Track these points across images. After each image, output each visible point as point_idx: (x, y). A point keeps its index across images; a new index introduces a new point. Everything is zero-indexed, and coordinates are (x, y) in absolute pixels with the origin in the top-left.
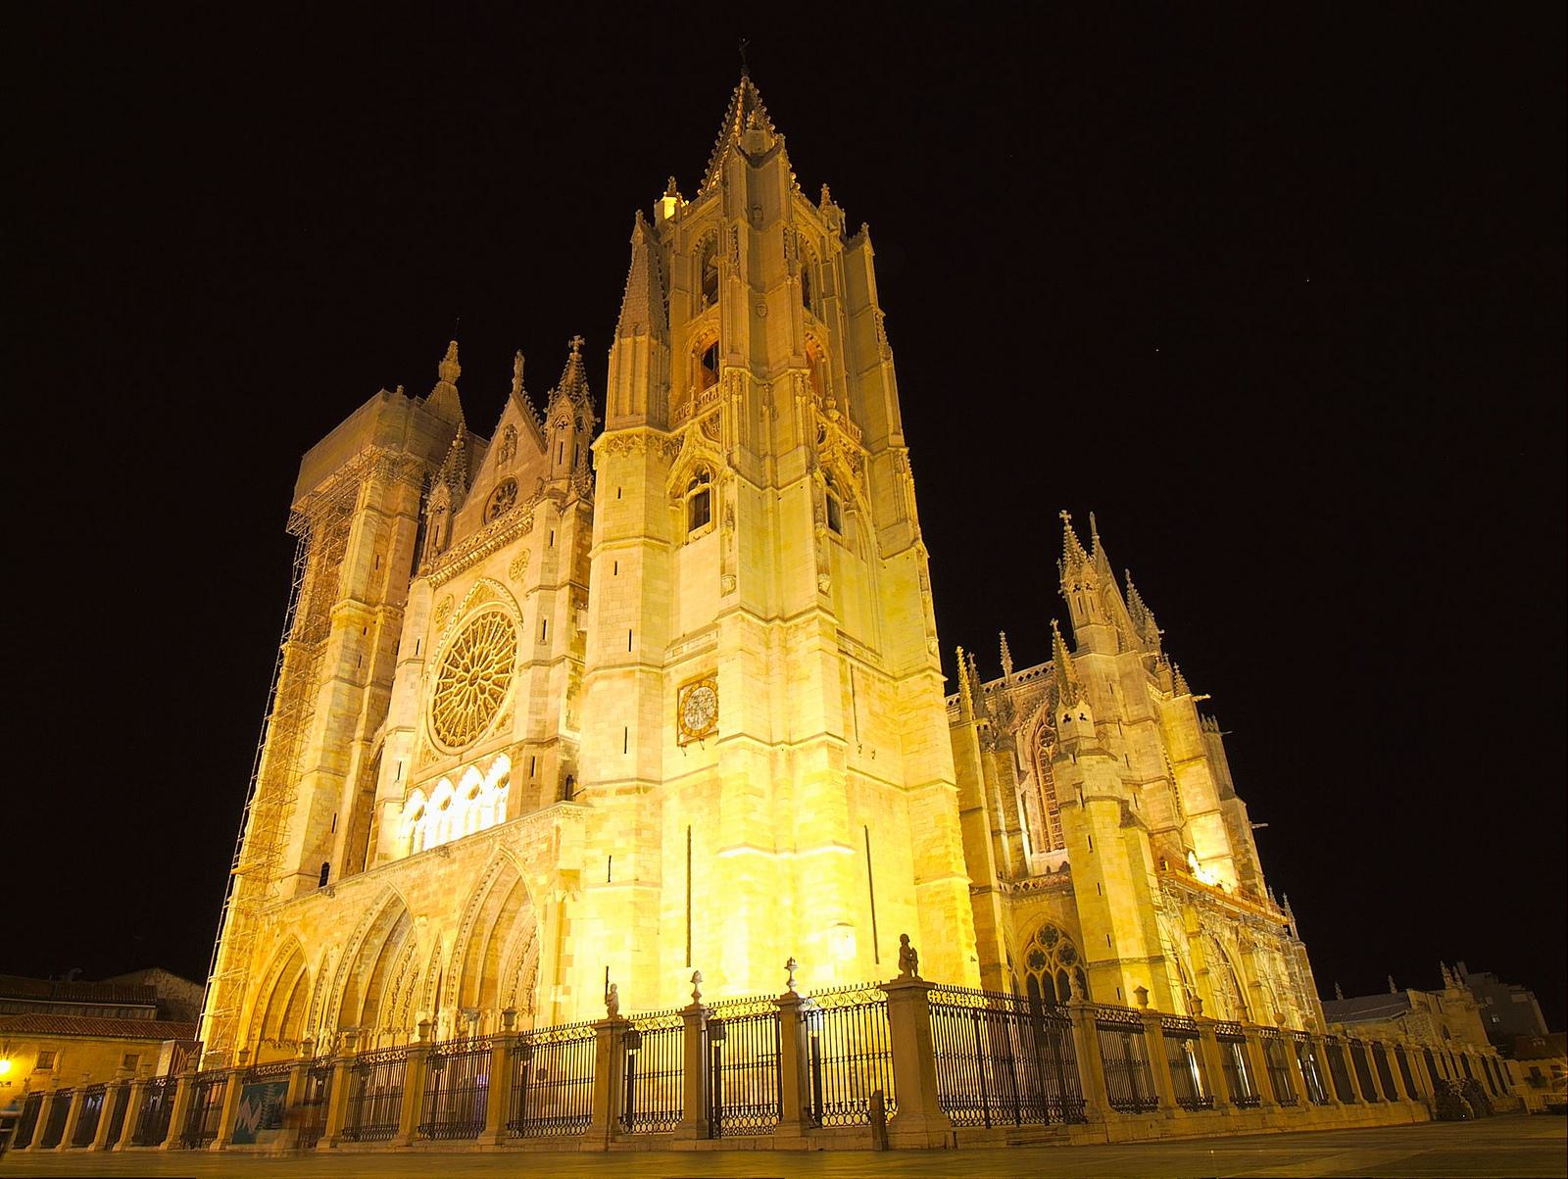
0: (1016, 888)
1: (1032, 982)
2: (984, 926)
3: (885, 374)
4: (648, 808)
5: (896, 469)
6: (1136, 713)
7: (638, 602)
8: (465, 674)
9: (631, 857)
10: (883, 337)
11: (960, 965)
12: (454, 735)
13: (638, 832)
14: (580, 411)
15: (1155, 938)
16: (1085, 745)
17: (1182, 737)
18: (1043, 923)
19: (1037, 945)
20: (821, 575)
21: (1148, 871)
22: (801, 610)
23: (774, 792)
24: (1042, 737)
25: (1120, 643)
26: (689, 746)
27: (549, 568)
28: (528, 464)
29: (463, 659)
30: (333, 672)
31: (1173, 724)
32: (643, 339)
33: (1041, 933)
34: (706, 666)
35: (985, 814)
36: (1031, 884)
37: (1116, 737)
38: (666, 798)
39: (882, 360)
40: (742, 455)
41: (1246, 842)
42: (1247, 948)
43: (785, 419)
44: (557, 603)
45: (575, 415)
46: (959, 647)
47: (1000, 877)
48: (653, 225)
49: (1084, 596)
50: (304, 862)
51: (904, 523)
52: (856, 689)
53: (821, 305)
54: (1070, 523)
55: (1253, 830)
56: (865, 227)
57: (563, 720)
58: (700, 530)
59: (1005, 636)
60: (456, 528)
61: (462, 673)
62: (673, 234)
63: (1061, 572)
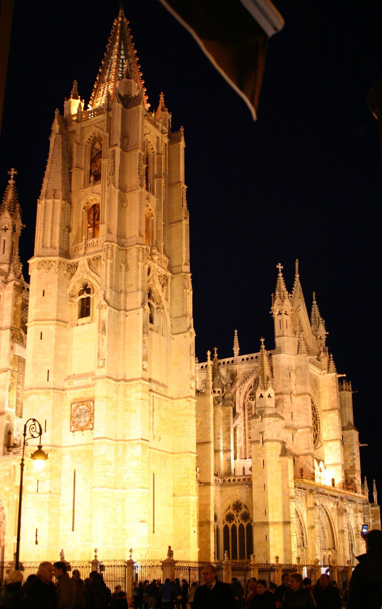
0: (224, 481)
1: (226, 528)
2: (204, 502)
3: (184, 228)
5: (184, 285)
6: (300, 389)
7: (52, 356)
10: (185, 204)
11: (189, 534)
13: (51, 470)
14: (15, 221)
15: (288, 513)
16: (268, 411)
17: (328, 397)
18: (235, 500)
19: (231, 511)
20: (144, 362)
21: (289, 480)
22: (134, 377)
24: (250, 395)
25: (298, 348)
26: (76, 432)
31: (324, 389)
32: (59, 202)
33: (234, 505)
34: (86, 394)
35: (212, 446)
36: (232, 480)
37: (288, 403)
39: (183, 219)
40: (111, 295)
41: (354, 454)
42: (341, 512)
43: (133, 272)
44: (3, 338)
46: (209, 351)
48: (63, 116)
49: (283, 319)
51: (185, 318)
52: (155, 407)
53: (153, 183)
54: (282, 272)
55: (360, 447)
56: (182, 129)
57: (7, 403)
58: (85, 320)
59: (238, 333)
62: (75, 127)
63: (273, 302)
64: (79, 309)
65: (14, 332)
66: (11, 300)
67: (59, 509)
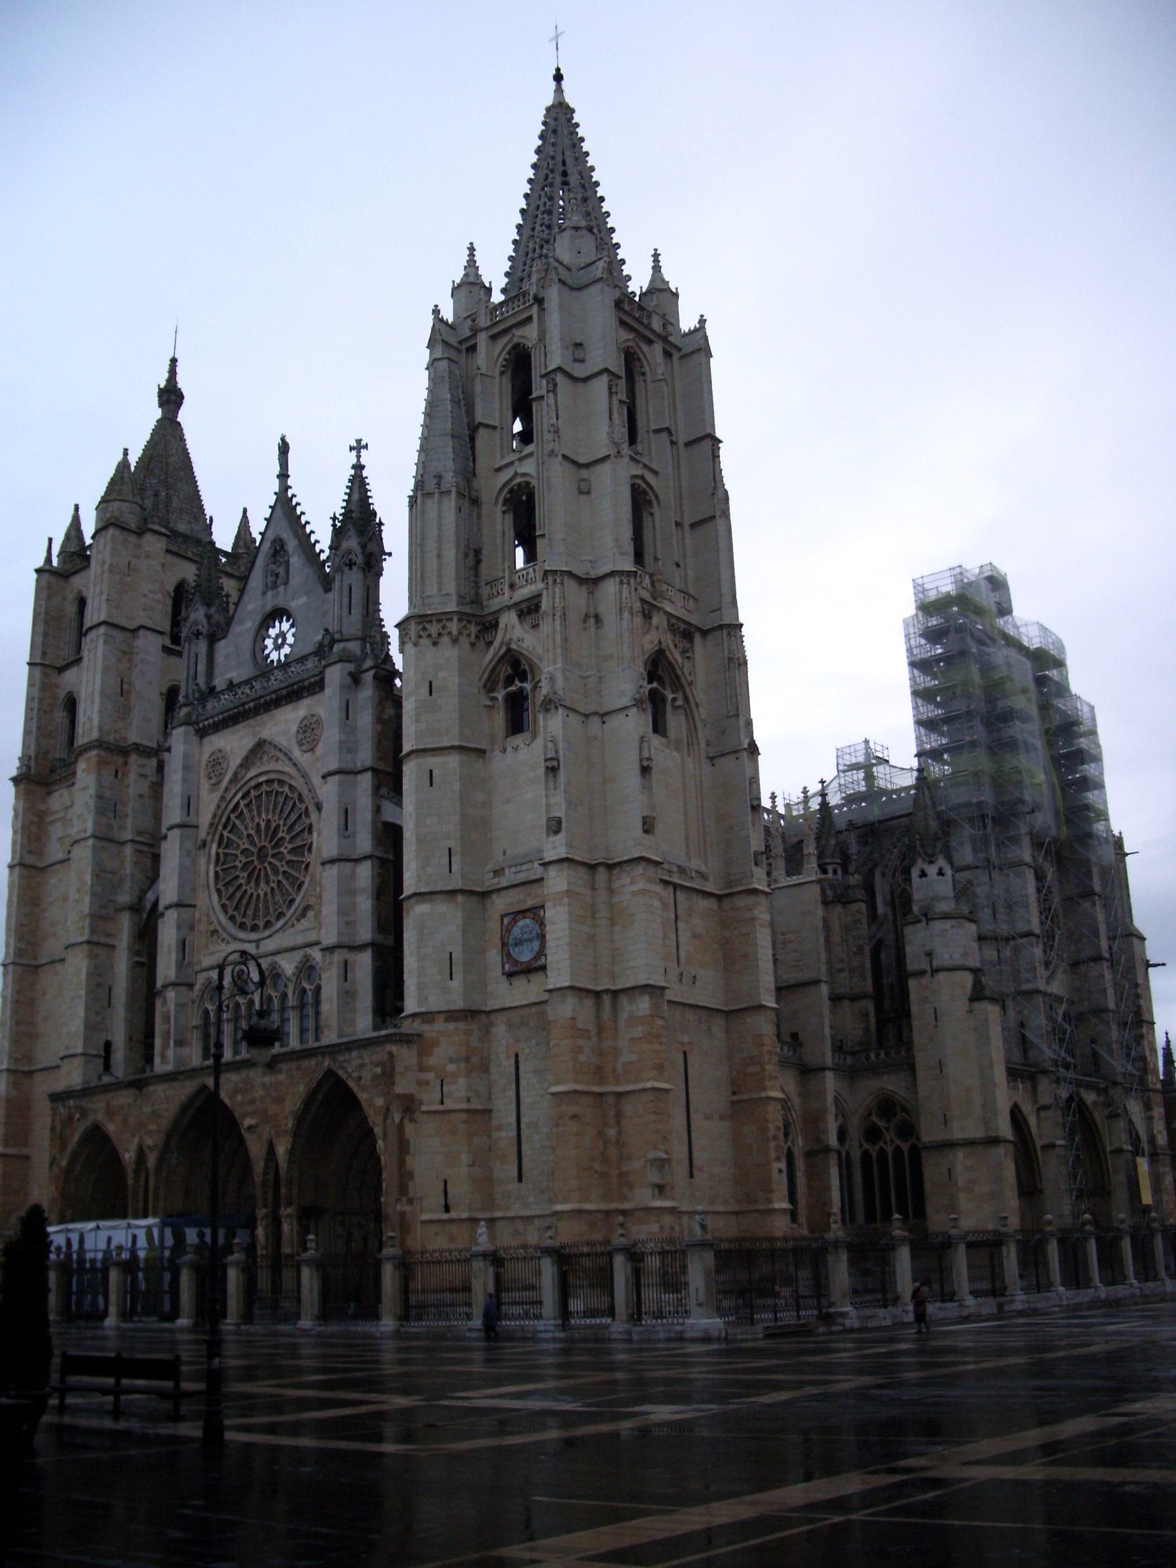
1: (866, 1155)
4: (476, 1032)
8: (251, 848)
9: (462, 1081)
12: (244, 915)
13: (467, 1059)
19: (875, 1119)
23: (599, 1033)
27: (347, 747)
28: (304, 599)
29: (246, 828)
30: (90, 826)
35: (824, 989)
38: (492, 1024)
40: (566, 679)
45: (363, 553)
47: (838, 1048)
50: (87, 1040)
52: (680, 912)
58: (519, 739)
60: (219, 658)
61: (246, 846)
64: (506, 714)
65: (381, 776)
66: (370, 711)
67: (490, 1136)
